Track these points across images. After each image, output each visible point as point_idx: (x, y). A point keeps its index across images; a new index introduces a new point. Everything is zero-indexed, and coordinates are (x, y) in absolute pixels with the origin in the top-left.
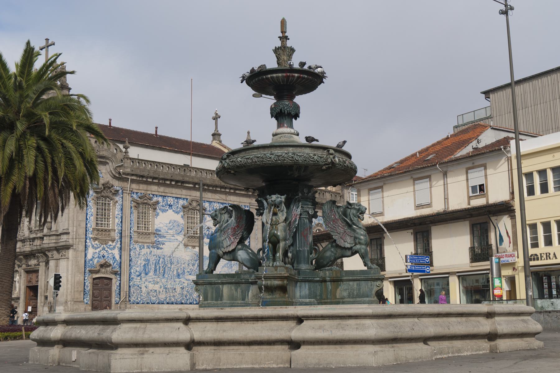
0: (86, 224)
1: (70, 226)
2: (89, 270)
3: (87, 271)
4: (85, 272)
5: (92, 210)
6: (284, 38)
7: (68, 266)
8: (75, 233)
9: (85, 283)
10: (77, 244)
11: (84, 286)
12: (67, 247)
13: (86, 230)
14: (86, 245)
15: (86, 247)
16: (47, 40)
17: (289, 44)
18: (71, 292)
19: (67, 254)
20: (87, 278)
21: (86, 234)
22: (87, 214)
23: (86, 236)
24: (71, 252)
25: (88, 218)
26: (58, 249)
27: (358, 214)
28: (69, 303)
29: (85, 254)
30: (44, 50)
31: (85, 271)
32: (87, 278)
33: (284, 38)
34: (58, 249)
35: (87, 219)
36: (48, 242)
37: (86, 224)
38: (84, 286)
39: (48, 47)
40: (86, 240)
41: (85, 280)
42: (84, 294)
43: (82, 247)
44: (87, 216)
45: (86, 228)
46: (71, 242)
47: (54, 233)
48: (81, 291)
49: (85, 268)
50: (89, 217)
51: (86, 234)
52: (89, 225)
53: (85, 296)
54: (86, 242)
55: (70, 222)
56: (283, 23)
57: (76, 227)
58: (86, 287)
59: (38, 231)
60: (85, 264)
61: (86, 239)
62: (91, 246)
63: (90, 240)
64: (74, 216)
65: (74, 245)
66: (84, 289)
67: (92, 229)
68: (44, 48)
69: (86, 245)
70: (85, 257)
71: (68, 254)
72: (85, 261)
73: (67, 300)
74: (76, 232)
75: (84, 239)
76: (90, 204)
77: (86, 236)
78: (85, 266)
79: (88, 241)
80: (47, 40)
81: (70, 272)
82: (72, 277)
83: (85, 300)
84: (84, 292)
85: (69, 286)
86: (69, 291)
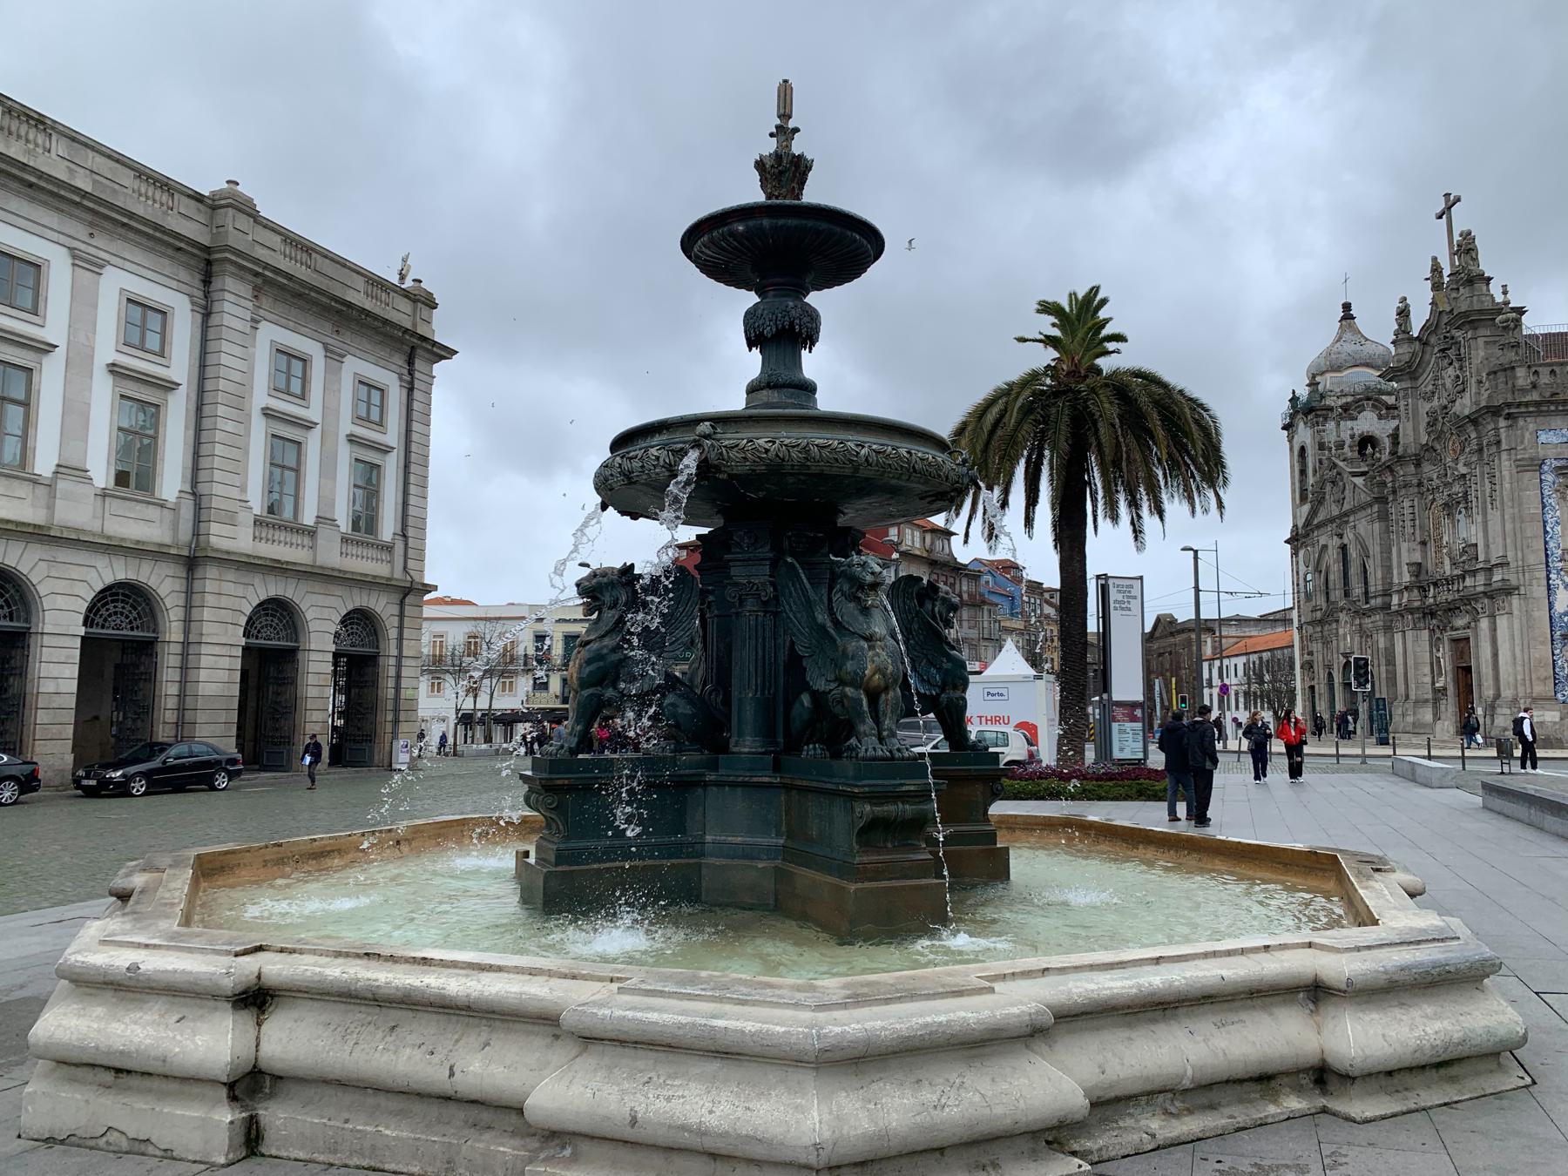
0: (1546, 543)
1: (1508, 548)
2: (1561, 635)
3: (1555, 637)
4: (1552, 640)
5: (1558, 513)
6: (784, 132)
7: (1511, 628)
8: (1520, 563)
9: (1554, 661)
10: (1527, 583)
11: (1554, 668)
12: (1508, 590)
13: (1547, 555)
14: (1549, 585)
15: (1549, 589)
16: (1447, 195)
17: (797, 148)
18: (1524, 680)
19: (1507, 605)
20: (1558, 651)
21: (1547, 562)
22: (1545, 522)
23: (1547, 566)
24: (1515, 601)
25: (1548, 529)
26: (1490, 595)
27: (854, 590)
28: (1522, 701)
29: (1550, 603)
30: (1444, 217)
31: (1552, 636)
32: (1558, 651)
33: (784, 132)
34: (1490, 595)
35: (1546, 532)
36: (1477, 583)
37: (1546, 543)
38: (1554, 668)
39: (1450, 208)
40: (1548, 576)
41: (1553, 655)
42: (1555, 684)
43: (1540, 591)
44: (1545, 527)
45: (1546, 550)
46: (1514, 582)
47: (1481, 565)
48: (1546, 679)
49: (1552, 631)
50: (1552, 529)
51: (1547, 562)
52: (1551, 544)
53: (1559, 687)
54: (1549, 579)
55: (1508, 541)
56: (785, 91)
57: (1522, 550)
58: (1557, 670)
59: (1464, 562)
60: (1551, 620)
61: (1549, 572)
62: (1561, 587)
63: (1558, 574)
64: (1514, 528)
65: (1522, 588)
66: (1555, 673)
67: (1560, 552)
68: (1444, 213)
69: (1549, 585)
70: (1550, 610)
71: (1511, 604)
72: (1551, 617)
73: (1517, 695)
74: (1523, 560)
75: (1544, 574)
76: (1550, 501)
77: (1547, 566)
78: (1551, 627)
79: (1553, 576)
80: (1447, 195)
81: (1517, 641)
82: (1522, 651)
83: (1559, 695)
84: (1555, 678)
85: (1519, 668)
86: (1519, 677)
